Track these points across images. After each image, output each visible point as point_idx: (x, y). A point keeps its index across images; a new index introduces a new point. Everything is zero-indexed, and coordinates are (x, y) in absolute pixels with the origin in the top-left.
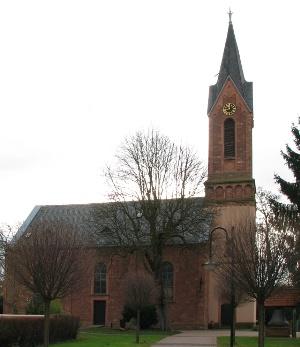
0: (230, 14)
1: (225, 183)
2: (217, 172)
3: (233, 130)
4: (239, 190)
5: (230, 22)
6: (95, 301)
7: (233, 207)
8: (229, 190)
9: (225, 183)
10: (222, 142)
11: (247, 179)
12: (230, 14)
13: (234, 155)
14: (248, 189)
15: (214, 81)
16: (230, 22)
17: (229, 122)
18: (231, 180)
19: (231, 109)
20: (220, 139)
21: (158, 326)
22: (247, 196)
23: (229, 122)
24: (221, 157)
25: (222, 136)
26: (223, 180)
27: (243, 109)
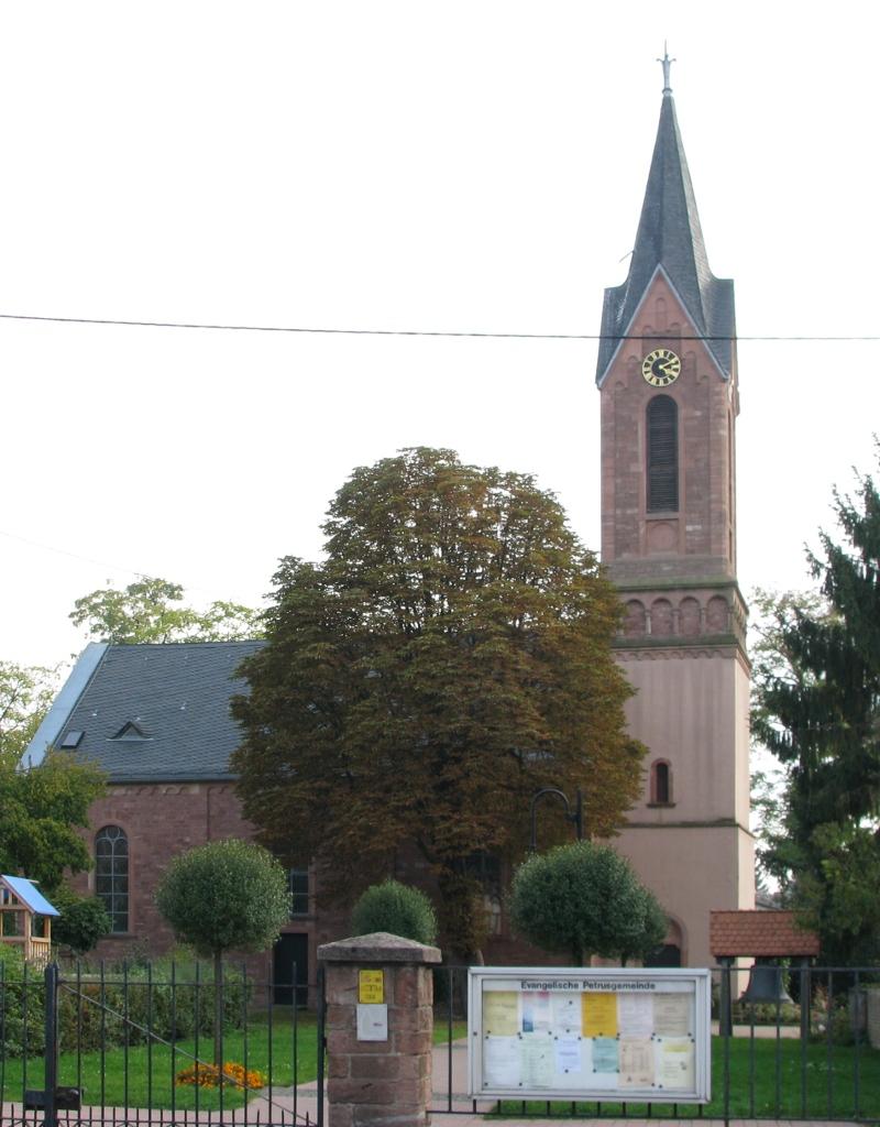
0: (666, 63)
1: (652, 590)
2: (626, 556)
3: (673, 432)
4: (690, 609)
5: (667, 90)
6: (127, 930)
7: (675, 662)
8: (663, 609)
9: (652, 590)
10: (640, 467)
11: (715, 579)
12: (666, 63)
13: (675, 508)
14: (717, 607)
15: (619, 275)
16: (667, 90)
17: (662, 409)
18: (669, 581)
19: (659, 373)
20: (634, 457)
21: (677, 945)
22: (713, 631)
23: (662, 409)
24: (639, 510)
25: (641, 447)
26: (648, 581)
27: (702, 370)
